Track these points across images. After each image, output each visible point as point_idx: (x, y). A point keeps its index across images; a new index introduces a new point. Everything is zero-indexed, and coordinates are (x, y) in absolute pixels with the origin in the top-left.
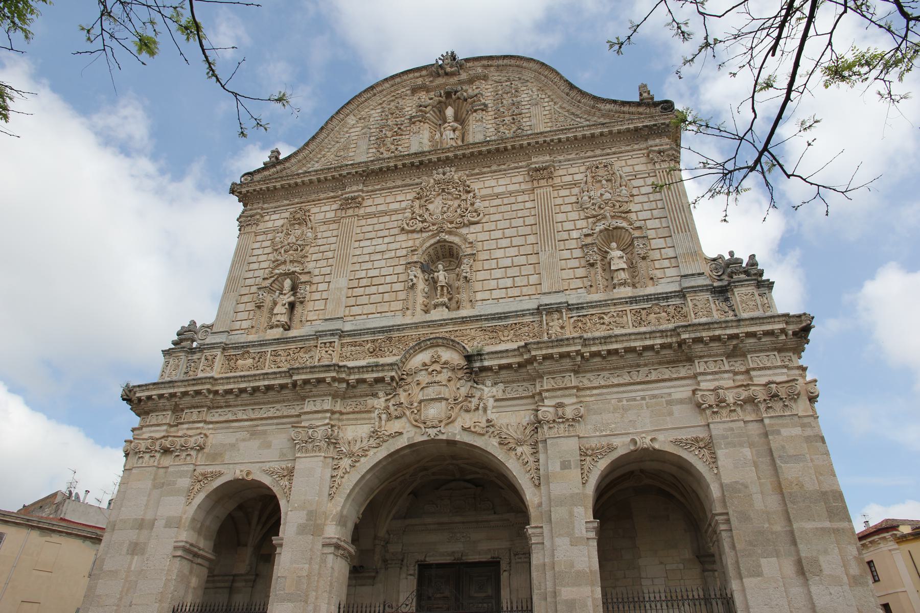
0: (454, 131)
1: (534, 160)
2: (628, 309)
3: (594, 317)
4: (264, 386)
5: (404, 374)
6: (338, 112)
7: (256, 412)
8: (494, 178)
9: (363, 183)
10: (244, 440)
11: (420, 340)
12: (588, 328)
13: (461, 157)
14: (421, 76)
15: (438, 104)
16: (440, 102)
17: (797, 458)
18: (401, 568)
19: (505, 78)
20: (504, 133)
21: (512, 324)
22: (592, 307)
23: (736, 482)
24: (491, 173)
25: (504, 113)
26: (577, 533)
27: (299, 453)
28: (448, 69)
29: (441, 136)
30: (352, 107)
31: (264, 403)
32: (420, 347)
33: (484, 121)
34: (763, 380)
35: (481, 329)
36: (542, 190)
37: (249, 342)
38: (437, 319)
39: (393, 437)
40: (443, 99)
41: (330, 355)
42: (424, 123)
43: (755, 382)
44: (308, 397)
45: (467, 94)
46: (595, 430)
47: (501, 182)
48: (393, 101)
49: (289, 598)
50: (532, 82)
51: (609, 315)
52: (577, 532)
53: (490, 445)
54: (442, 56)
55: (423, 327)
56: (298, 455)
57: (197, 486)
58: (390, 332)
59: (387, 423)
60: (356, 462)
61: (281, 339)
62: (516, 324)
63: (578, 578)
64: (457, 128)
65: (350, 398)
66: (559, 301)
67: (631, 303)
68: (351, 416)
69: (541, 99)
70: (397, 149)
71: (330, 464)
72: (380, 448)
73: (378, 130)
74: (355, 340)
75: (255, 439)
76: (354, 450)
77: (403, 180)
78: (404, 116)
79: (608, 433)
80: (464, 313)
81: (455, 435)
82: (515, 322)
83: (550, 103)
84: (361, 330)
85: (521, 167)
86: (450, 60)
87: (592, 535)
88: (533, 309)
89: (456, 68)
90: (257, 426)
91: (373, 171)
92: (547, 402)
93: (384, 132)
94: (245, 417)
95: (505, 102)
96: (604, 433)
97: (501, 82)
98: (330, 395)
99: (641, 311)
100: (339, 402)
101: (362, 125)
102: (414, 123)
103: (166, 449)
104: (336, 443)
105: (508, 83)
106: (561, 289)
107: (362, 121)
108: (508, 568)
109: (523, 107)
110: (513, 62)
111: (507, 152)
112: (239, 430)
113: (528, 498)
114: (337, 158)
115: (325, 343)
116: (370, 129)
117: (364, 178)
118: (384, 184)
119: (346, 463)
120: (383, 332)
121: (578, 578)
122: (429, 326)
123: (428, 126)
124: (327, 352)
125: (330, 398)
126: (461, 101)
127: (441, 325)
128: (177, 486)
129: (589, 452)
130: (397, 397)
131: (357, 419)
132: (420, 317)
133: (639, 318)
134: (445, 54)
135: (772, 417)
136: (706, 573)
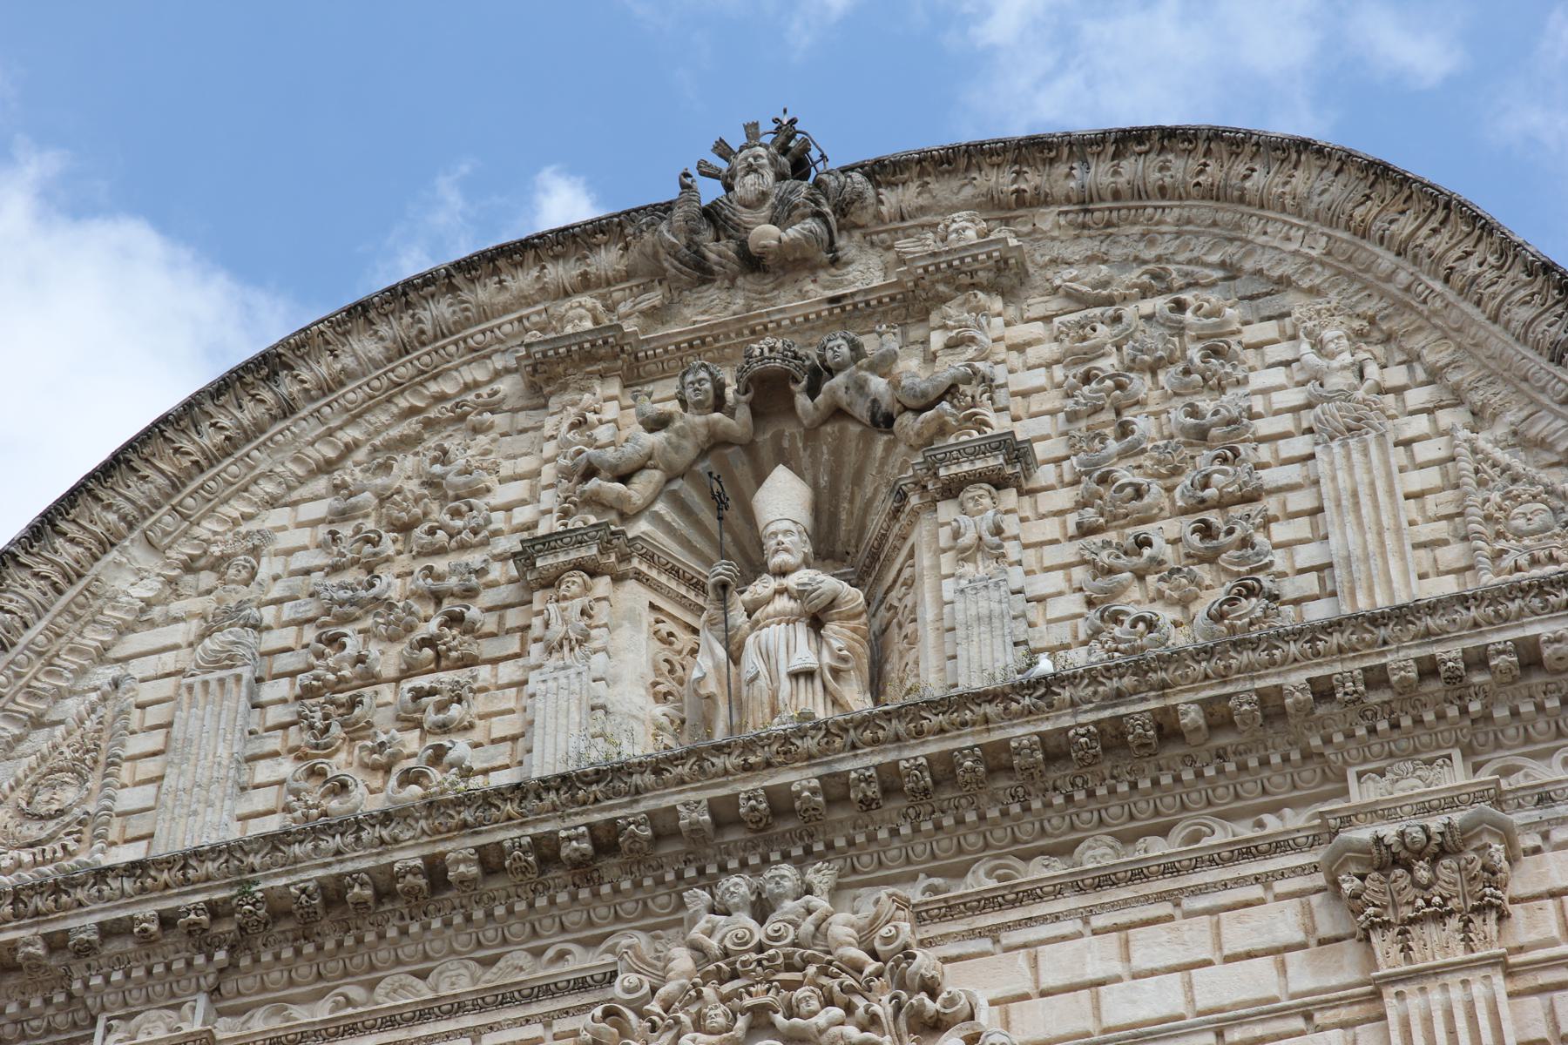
0: (816, 623)
1: (1361, 793)
6: (44, 527)
8: (1098, 921)
9: (215, 992)
13: (873, 790)
14: (586, 283)
15: (703, 454)
16: (716, 443)
19: (1135, 275)
20: (1151, 625)
24: (1080, 889)
25: (1139, 493)
28: (765, 234)
29: (735, 657)
30: (137, 491)
33: (1013, 551)
36: (1436, 996)
40: (738, 423)
42: (618, 579)
45: (895, 385)
47: (1152, 947)
48: (407, 443)
50: (1314, 291)
54: (723, 150)
64: (832, 603)
69: (1382, 391)
70: (438, 755)
73: (310, 634)
77: (488, 963)
78: (482, 536)
83: (1446, 418)
85: (1279, 846)
86: (769, 176)
89: (811, 224)
91: (279, 909)
93: (353, 644)
95: (1143, 425)
97: (1109, 301)
101: (208, 604)
102: (550, 582)
105: (1159, 304)
107: (207, 579)
109: (1265, 453)
110: (1180, 168)
111: (1174, 751)
114: (33, 831)
116: (258, 627)
117: (221, 956)
118: (356, 993)
123: (644, 596)
126: (854, 429)
134: (736, 140)
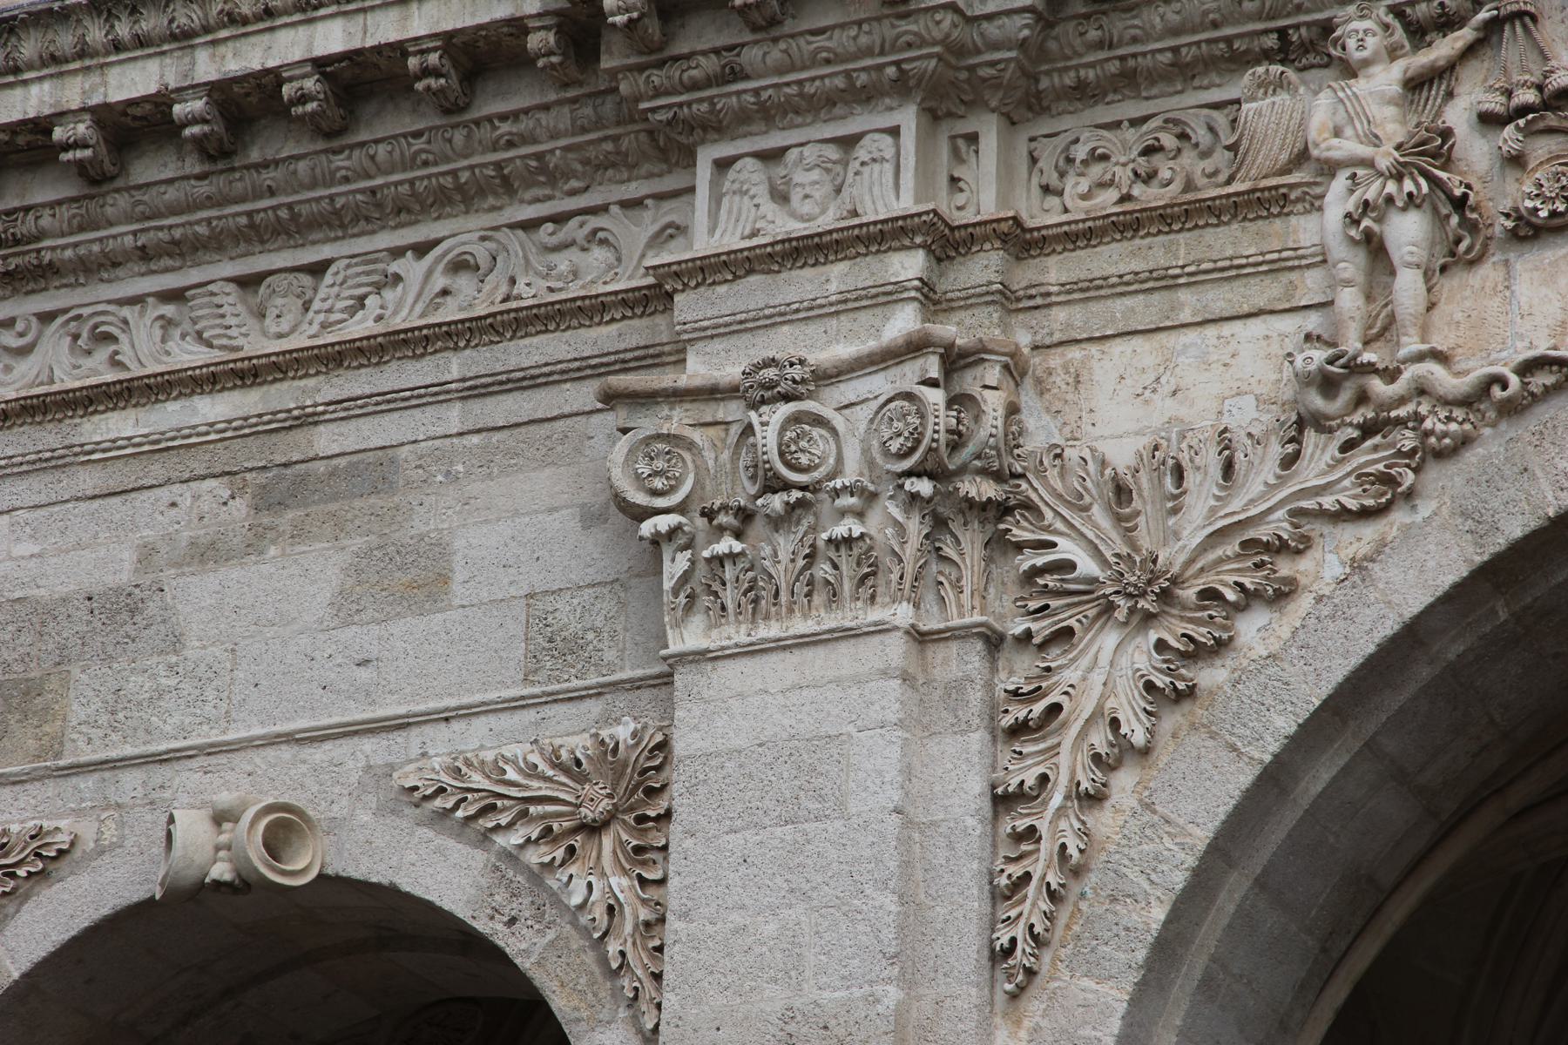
4: (320, 64)
7: (284, 305)
10: (206, 554)
27: (697, 621)
31: (338, 222)
39: (1512, 409)
44: (714, 127)
56: (691, 636)
59: (1448, 286)
60: (1197, 653)
65: (1084, 93)
68: (1111, 259)
71: (976, 696)
72: (1399, 516)
75: (299, 534)
76: (1172, 556)
90: (305, 420)
94: (188, 355)
98: (902, 87)
100: (990, 142)
104: (1003, 510)
112: (157, 470)
125: (907, 118)
130: (1512, 47)
131: (1164, 281)
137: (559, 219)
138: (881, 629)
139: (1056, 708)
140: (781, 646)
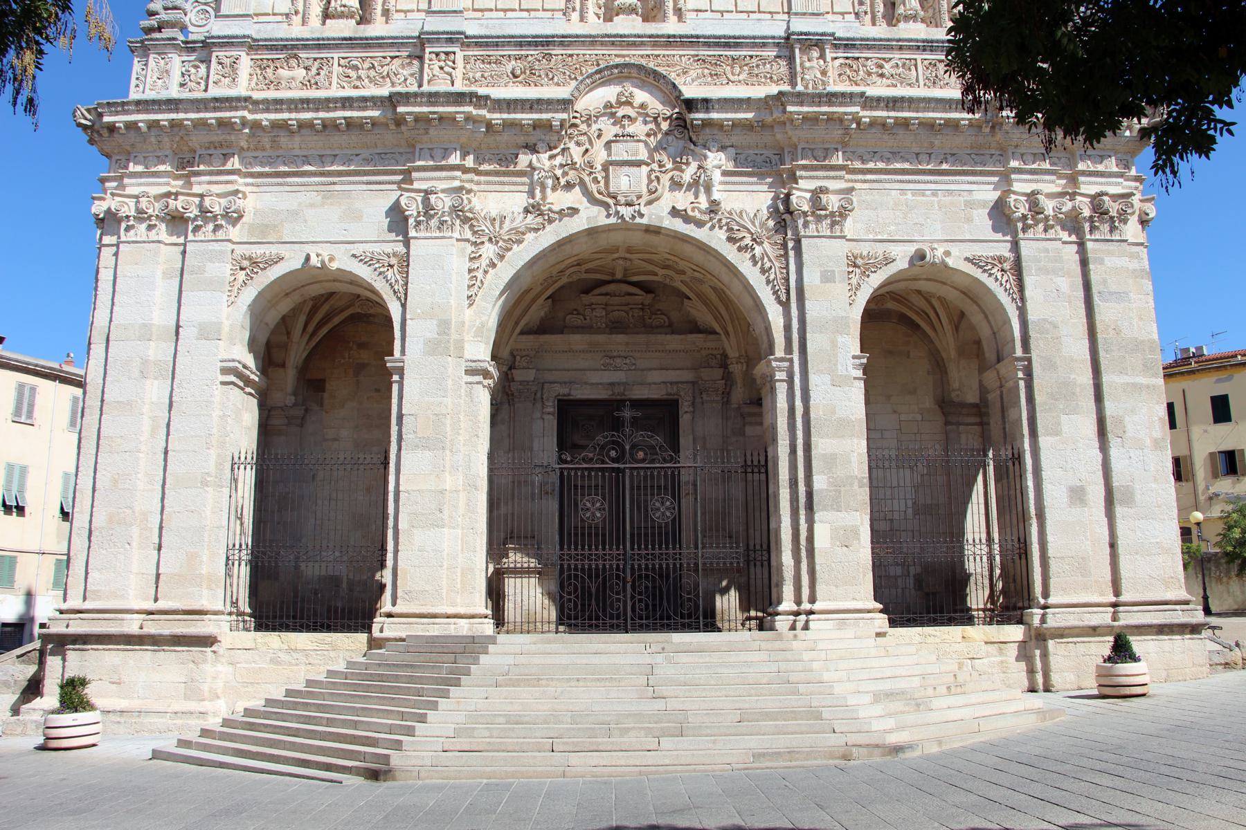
2: (919, 57)
3: (869, 63)
5: (576, 118)
10: (312, 205)
11: (598, 65)
12: (860, 78)
17: (1120, 296)
18: (534, 404)
21: (745, 57)
22: (869, 48)
23: (1044, 320)
26: (841, 370)
32: (606, 75)
34: (1093, 190)
35: (696, 58)
37: (298, 40)
38: (626, 32)
41: (447, 73)
43: (1082, 191)
46: (868, 232)
49: (425, 444)
51: (892, 63)
52: (840, 367)
53: (716, 239)
55: (603, 44)
57: (242, 276)
58: (548, 46)
61: (356, 39)
62: (751, 57)
63: (842, 427)
66: (820, 30)
67: (924, 50)
74: (488, 53)
75: (332, 204)
79: (885, 237)
80: (671, 26)
81: (661, 218)
82: (750, 53)
84: (498, 37)
87: (859, 373)
88: (780, 38)
92: (802, 184)
96: (880, 237)
99: (938, 64)
103: (175, 214)
106: (822, 11)
108: (691, 409)
112: (302, 188)
113: (770, 319)
115: (437, 54)
119: (489, 251)
120: (536, 44)
121: (842, 427)
122: (613, 43)
124: (441, 68)
127: (633, 45)
128: (206, 275)
129: (859, 262)
131: (503, 184)
132: (594, 25)
133: (934, 75)
135: (1097, 240)
136: (949, 427)
137: (386, 154)
138: (451, 237)
139: (481, 255)
140: (431, 238)
